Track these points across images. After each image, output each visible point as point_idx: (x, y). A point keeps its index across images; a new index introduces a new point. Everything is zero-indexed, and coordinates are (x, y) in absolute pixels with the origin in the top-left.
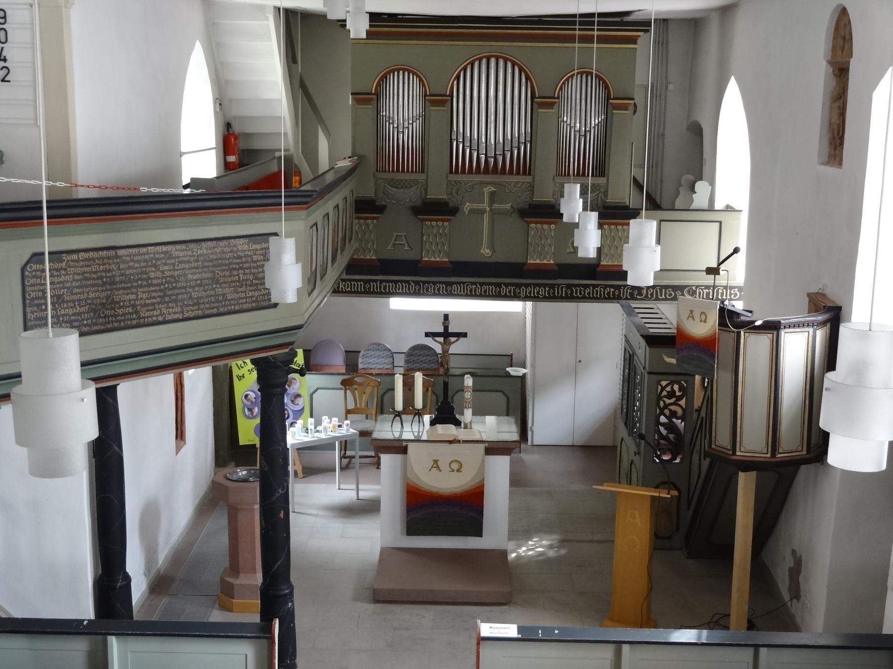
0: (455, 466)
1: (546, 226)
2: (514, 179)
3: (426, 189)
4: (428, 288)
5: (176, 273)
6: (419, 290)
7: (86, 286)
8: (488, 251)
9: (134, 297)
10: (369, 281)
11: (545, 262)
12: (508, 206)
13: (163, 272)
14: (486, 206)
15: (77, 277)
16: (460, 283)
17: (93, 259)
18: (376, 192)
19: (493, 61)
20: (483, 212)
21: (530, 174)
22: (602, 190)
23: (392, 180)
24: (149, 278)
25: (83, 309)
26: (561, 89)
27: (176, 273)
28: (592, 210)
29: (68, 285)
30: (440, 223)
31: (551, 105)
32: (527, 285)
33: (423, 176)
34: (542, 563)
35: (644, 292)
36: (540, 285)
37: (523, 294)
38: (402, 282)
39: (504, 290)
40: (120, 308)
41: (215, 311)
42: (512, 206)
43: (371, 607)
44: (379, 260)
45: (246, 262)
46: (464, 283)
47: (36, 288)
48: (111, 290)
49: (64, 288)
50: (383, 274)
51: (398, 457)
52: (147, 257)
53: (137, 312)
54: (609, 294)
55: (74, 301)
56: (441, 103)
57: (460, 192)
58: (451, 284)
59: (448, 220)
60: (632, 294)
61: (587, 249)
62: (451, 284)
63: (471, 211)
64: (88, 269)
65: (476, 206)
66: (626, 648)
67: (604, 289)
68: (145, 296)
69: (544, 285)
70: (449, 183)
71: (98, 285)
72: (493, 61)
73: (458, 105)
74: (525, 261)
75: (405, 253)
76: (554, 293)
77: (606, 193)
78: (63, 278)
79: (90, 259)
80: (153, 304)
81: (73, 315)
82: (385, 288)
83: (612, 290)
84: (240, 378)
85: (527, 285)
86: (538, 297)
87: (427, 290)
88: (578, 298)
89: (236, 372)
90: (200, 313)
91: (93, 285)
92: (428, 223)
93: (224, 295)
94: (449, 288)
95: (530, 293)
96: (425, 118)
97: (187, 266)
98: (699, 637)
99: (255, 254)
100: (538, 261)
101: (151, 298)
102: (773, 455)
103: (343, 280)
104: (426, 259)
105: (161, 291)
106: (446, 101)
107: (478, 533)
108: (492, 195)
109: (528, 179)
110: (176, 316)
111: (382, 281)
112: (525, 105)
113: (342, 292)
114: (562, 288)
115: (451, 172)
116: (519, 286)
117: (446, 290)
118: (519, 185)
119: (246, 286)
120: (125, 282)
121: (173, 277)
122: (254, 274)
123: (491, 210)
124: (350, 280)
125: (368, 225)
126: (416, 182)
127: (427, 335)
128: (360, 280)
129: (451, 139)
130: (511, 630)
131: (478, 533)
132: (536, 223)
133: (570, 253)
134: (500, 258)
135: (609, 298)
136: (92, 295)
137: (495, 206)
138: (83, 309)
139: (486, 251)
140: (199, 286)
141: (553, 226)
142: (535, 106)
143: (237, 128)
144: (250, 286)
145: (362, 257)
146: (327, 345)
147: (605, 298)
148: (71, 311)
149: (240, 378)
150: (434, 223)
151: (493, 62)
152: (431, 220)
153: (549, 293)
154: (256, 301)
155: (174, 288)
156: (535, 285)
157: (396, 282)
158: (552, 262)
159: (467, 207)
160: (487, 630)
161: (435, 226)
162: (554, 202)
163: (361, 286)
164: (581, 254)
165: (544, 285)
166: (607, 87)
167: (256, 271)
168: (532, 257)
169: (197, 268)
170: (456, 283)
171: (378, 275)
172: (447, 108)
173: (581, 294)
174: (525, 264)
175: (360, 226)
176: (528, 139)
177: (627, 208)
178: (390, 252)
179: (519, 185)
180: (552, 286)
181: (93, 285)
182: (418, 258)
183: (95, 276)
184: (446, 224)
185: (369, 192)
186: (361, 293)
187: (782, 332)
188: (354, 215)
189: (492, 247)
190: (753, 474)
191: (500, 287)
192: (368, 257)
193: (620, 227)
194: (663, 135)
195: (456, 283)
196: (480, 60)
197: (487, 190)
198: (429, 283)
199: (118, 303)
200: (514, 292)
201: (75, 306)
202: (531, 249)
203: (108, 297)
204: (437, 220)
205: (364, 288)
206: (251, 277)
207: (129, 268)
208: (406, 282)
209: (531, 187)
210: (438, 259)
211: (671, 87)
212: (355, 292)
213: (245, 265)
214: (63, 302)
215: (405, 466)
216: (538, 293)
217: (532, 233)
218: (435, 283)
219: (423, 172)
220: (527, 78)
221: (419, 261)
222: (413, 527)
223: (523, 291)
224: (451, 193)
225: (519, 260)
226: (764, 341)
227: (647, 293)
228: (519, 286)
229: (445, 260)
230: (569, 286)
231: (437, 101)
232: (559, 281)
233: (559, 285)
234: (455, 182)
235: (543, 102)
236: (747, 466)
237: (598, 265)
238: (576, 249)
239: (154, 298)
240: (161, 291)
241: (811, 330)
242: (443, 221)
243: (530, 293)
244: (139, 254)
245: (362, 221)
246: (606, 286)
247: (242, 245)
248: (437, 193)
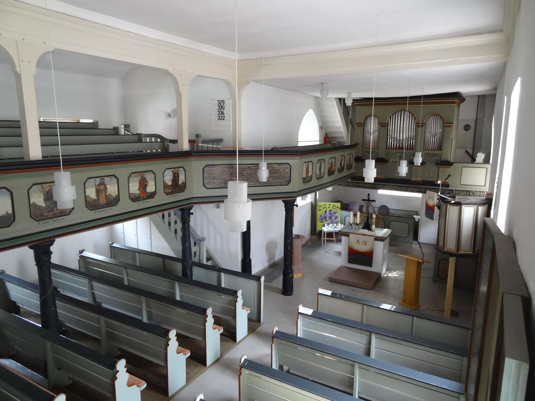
0: (364, 243)
19: (403, 112)
28: (372, 159)
34: (395, 279)
36: (415, 187)
39: (402, 188)
43: (329, 283)
51: (347, 238)
56: (384, 126)
58: (384, 185)
61: (402, 173)
62: (384, 185)
63: (393, 162)
65: (395, 160)
66: (365, 306)
69: (417, 188)
70: (386, 152)
72: (403, 112)
73: (390, 127)
77: (441, 156)
84: (320, 210)
89: (318, 208)
96: (379, 130)
98: (392, 308)
102: (458, 251)
107: (370, 265)
112: (414, 126)
127: (362, 200)
130: (329, 293)
131: (370, 265)
143: (330, 135)
146: (354, 203)
149: (320, 210)
159: (391, 160)
160: (321, 291)
163: (356, 184)
164: (400, 175)
165: (417, 188)
166: (443, 120)
172: (386, 128)
177: (449, 162)
180: (419, 188)
185: (360, 154)
187: (463, 206)
190: (455, 258)
194: (481, 137)
196: (398, 111)
197: (399, 155)
211: (485, 120)
215: (349, 241)
217: (413, 169)
220: (415, 118)
222: (350, 261)
223: (409, 189)
226: (456, 209)
231: (383, 125)
232: (422, 186)
235: (420, 125)
236: (451, 255)
238: (399, 173)
241: (476, 206)
247: (276, 166)
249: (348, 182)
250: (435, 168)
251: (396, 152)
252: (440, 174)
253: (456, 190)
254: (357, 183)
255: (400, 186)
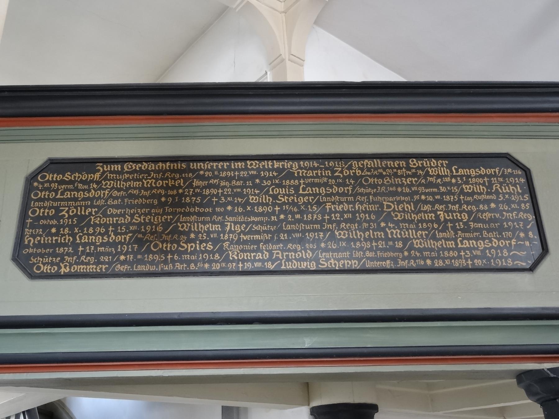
5: (302, 200)
7: (131, 207)
9: (216, 227)
13: (275, 197)
15: (115, 193)
17: (148, 172)
24: (247, 203)
25: (120, 238)
27: (302, 200)
29: (101, 202)
40: (189, 241)
41: (388, 264)
45: (450, 193)
47: (46, 204)
48: (174, 214)
49: (92, 206)
52: (243, 174)
53: (221, 251)
55: (106, 226)
64: (137, 184)
68: (238, 228)
71: (152, 206)
78: (92, 193)
79: (141, 171)
80: (257, 242)
81: (102, 245)
90: (355, 264)
91: (142, 206)
93: (405, 241)
97: (323, 190)
99: (467, 183)
101: (251, 232)
105: (273, 223)
110: (304, 266)
119: (455, 230)
120: (200, 205)
121: (294, 204)
122: (470, 213)
136: (137, 219)
138: (120, 238)
140: (352, 221)
144: (463, 231)
148: (99, 240)
154: (483, 256)
155: (299, 221)
167: (474, 208)
169: (343, 194)
181: (142, 206)
183: (147, 194)
199: (188, 233)
201: (107, 233)
203: (166, 224)
206: (465, 217)
207: (210, 186)
213: (447, 198)
214: (88, 225)
239: (258, 232)
240: (273, 223)
244: (229, 169)
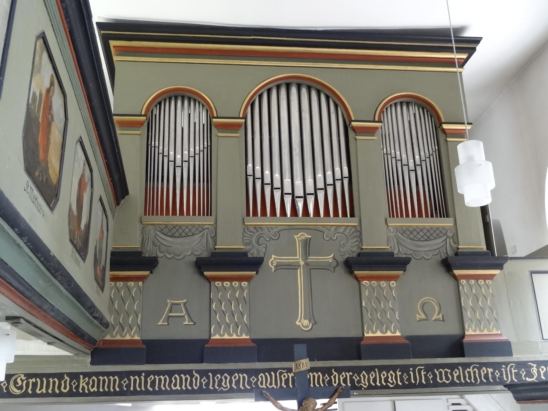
1: (383, 284)
2: (332, 222)
3: (215, 239)
4: (221, 380)
6: (207, 384)
8: (306, 322)
10: (128, 374)
11: (389, 334)
12: (329, 258)
14: (299, 258)
16: (269, 371)
18: (143, 243)
20: (294, 267)
21: (352, 215)
22: (450, 235)
23: (166, 226)
26: (382, 111)
30: (236, 284)
31: (371, 131)
32: (369, 369)
33: (207, 221)
35: (534, 370)
36: (387, 368)
37: (364, 383)
38: (180, 372)
42: (334, 258)
44: (144, 342)
46: (275, 370)
50: (148, 362)
54: (486, 376)
57: (261, 241)
59: (248, 279)
60: (518, 375)
62: (256, 372)
63: (278, 267)
67: (479, 369)
69: (394, 368)
70: (246, 228)
74: (360, 335)
75: (185, 329)
76: (409, 379)
77: (456, 238)
82: (153, 384)
83: (490, 370)
85: (369, 369)
86: (387, 387)
87: (220, 385)
88: (444, 385)
92: (218, 284)
94: (253, 379)
95: (375, 380)
100: (379, 334)
103: (85, 375)
104: (217, 337)
106: (238, 126)
108: (306, 244)
109: (353, 222)
111: (148, 373)
113: (83, 395)
114: (420, 371)
115: (248, 214)
116: (357, 370)
117: (249, 383)
118: (342, 230)
123: (307, 264)
124: (97, 374)
125: (129, 289)
126: (201, 229)
128: (113, 374)
129: (247, 176)
132: (370, 278)
133: (421, 320)
134: (325, 331)
135: (488, 383)
137: (312, 259)
139: (303, 324)
141: (393, 283)
142: (351, 134)
145: (118, 338)
147: (482, 383)
150: (227, 284)
151: (294, 91)
152: (223, 279)
153: (402, 380)
156: (381, 368)
157: (170, 373)
158: (398, 334)
159: (272, 261)
161: (231, 290)
162: (390, 250)
165: (394, 368)
168: (370, 328)
170: (264, 371)
171: (141, 363)
173: (447, 379)
174: (362, 338)
175: (118, 290)
176: (346, 173)
178: (162, 329)
179: (342, 230)
180: (405, 369)
182: (205, 336)
184: (244, 284)
185: (132, 243)
186: (115, 394)
188: (109, 273)
189: (311, 316)
191: (330, 374)
192: (128, 337)
193: (481, 282)
195: (264, 371)
197: (300, 237)
198: (222, 372)
200: (352, 381)
202: (367, 316)
204: (231, 279)
205: (120, 386)
208: (185, 372)
209: (359, 232)
210: (234, 337)
212: (105, 394)
216: (386, 380)
217: (366, 293)
218: (231, 372)
219: (209, 212)
221: (207, 341)
223: (364, 379)
224: (250, 243)
225: (353, 333)
227: (539, 372)
228: (357, 370)
229: (244, 337)
230: (429, 368)
233: (414, 366)
234: (255, 227)
237: (463, 336)
242: (240, 279)
243: (375, 380)
245: (120, 284)
246: (482, 365)
248: (230, 242)
249: (74, 376)
250: (443, 282)
251: (291, 228)
252: (467, 302)
253: (539, 363)
254: (122, 375)
255: (327, 371)
